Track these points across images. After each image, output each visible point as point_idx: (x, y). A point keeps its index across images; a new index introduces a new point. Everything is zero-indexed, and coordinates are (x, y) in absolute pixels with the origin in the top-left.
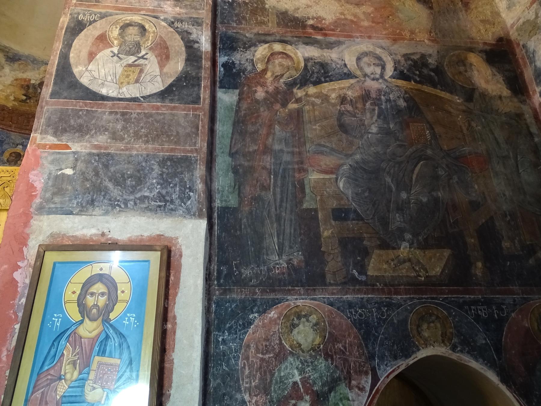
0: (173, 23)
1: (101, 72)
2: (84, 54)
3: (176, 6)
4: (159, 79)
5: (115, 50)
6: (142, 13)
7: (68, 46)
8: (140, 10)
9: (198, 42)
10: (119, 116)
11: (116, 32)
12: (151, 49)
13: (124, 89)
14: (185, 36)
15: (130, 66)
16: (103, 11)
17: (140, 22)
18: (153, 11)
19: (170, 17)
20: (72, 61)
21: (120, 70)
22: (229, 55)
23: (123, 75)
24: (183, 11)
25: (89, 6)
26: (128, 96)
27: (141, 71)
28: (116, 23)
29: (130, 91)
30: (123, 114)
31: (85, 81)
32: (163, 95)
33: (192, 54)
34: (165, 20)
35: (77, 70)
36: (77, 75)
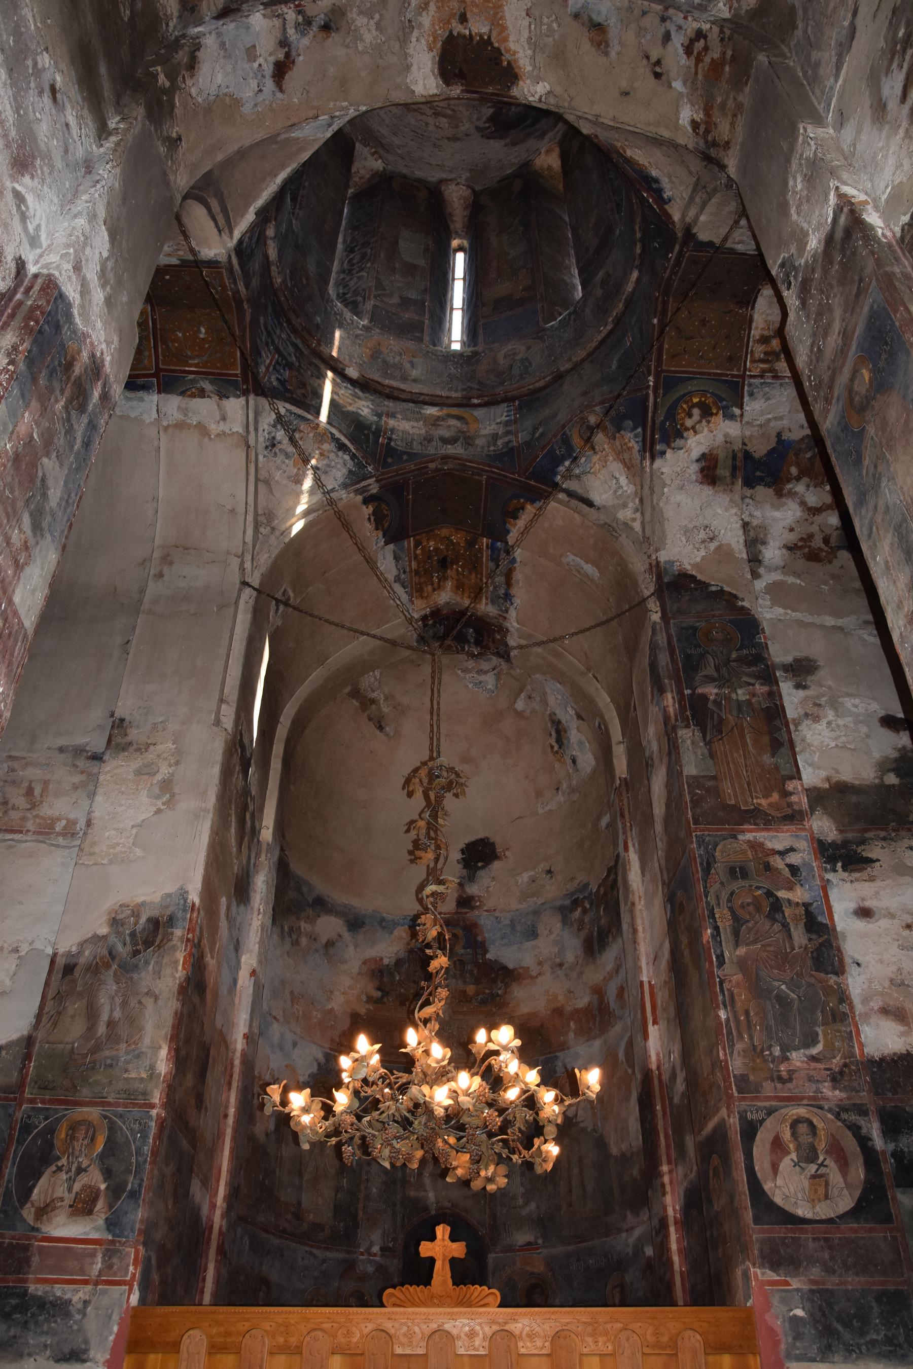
0: (839, 1114)
1: (788, 1186)
2: (767, 1165)
3: (834, 1088)
4: (845, 1192)
5: (794, 1156)
6: (805, 1102)
7: (749, 1155)
8: (802, 1098)
9: (871, 1139)
10: (822, 1242)
11: (787, 1135)
12: (827, 1152)
13: (818, 1209)
14: (855, 1129)
15: (813, 1177)
16: (767, 1104)
17: (807, 1116)
18: (814, 1098)
19: (832, 1104)
20: (759, 1175)
21: (806, 1183)
22: (895, 1141)
23: (810, 1189)
24: (844, 1095)
25: (752, 1099)
26: (824, 1217)
27: (827, 1184)
28: (783, 1121)
29: (824, 1211)
30: (827, 1240)
31: (778, 1200)
32: (855, 1213)
33: (870, 1157)
34: (830, 1110)
35: (767, 1186)
36: (769, 1193)
